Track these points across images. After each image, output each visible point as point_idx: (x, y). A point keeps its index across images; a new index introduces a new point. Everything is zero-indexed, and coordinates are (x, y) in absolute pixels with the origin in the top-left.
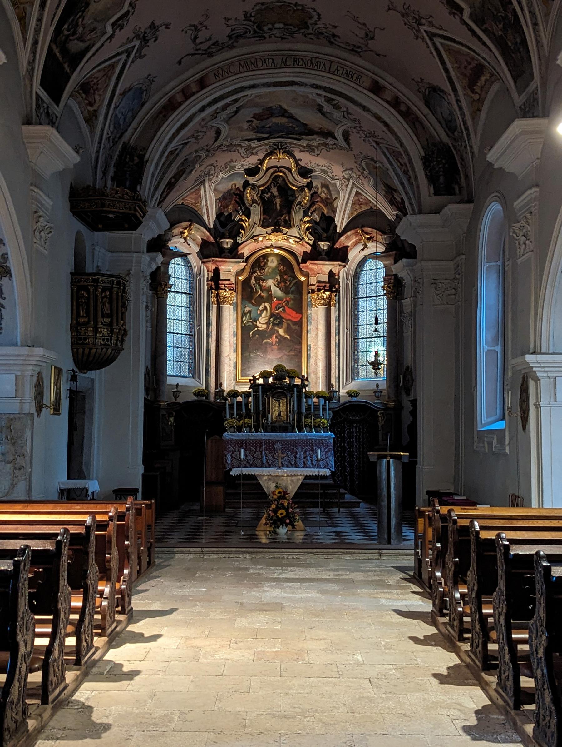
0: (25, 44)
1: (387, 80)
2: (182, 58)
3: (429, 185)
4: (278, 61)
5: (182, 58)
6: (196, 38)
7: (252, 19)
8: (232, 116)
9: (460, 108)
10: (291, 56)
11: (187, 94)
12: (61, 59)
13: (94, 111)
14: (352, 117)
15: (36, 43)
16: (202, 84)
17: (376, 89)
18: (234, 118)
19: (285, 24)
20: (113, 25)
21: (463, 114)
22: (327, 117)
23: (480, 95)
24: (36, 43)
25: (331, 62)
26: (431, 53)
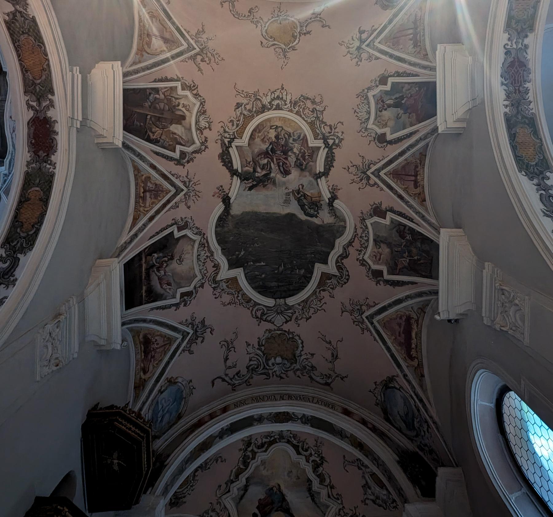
0: (130, 231)
1: (352, 407)
2: (216, 379)
3: (414, 487)
4: (278, 397)
5: (216, 379)
6: (226, 359)
7: (263, 348)
8: (242, 498)
9: (409, 382)
10: (286, 394)
11: (212, 416)
12: (143, 278)
13: (145, 380)
14: (335, 492)
15: (136, 235)
16: (225, 410)
17: (347, 412)
18: (243, 500)
19: (282, 359)
20: (183, 295)
21: (413, 387)
22: (316, 503)
23: (417, 358)
24: (136, 235)
25: (313, 397)
26: (375, 340)
